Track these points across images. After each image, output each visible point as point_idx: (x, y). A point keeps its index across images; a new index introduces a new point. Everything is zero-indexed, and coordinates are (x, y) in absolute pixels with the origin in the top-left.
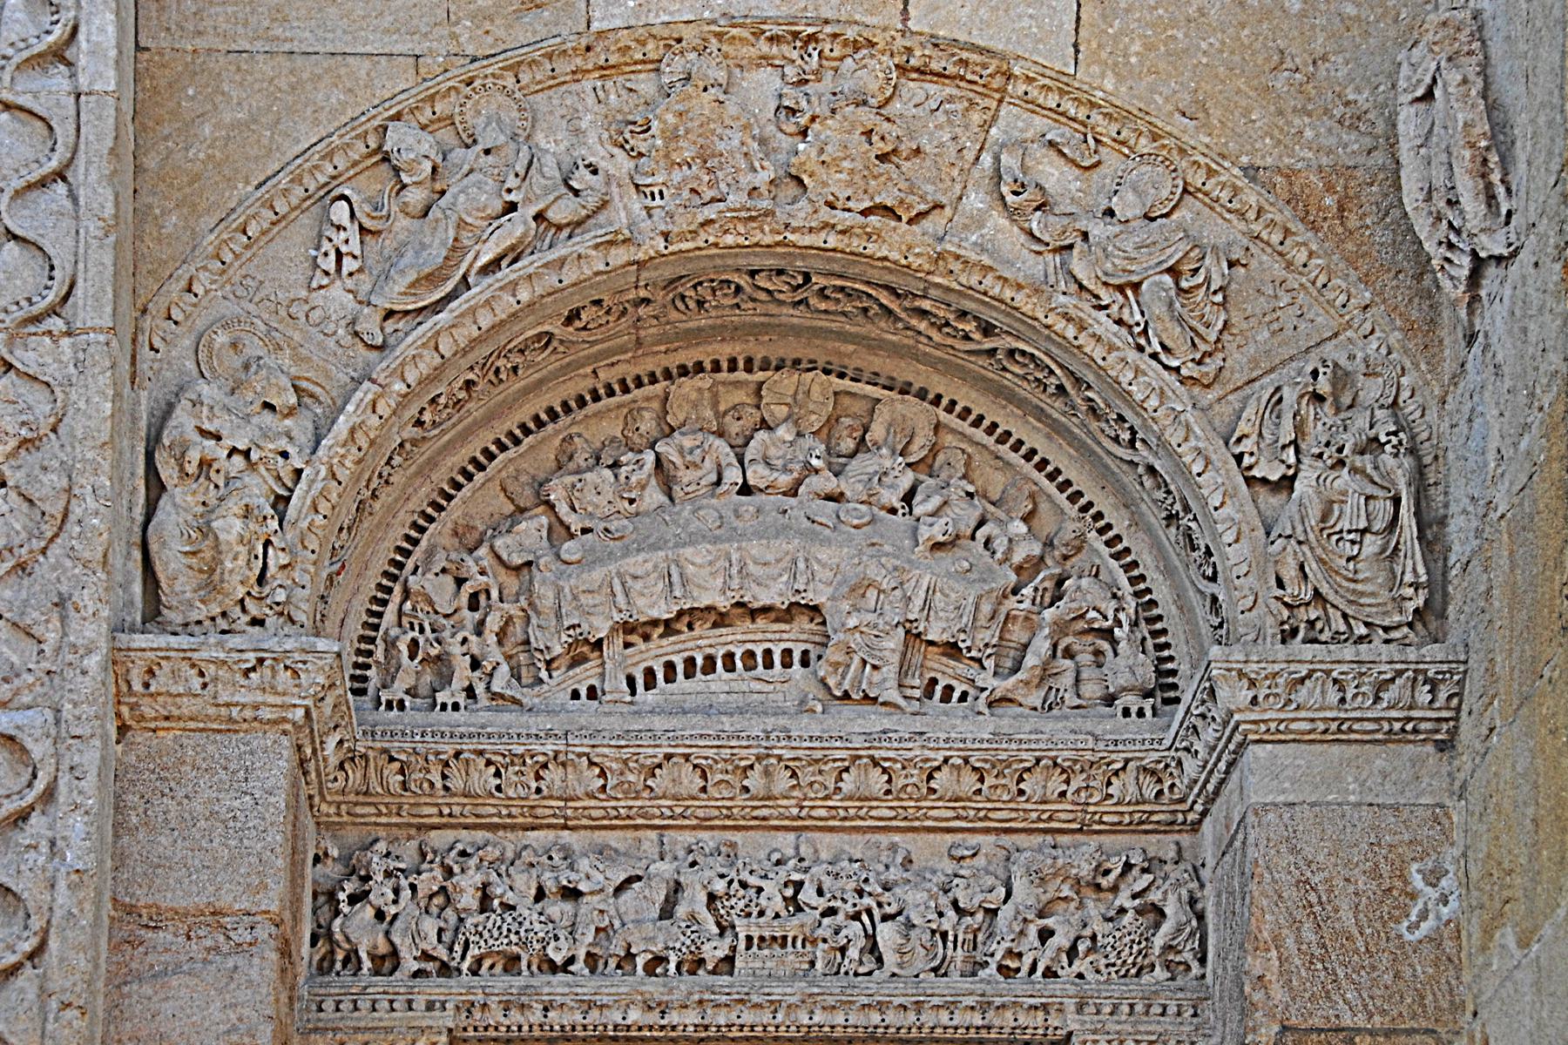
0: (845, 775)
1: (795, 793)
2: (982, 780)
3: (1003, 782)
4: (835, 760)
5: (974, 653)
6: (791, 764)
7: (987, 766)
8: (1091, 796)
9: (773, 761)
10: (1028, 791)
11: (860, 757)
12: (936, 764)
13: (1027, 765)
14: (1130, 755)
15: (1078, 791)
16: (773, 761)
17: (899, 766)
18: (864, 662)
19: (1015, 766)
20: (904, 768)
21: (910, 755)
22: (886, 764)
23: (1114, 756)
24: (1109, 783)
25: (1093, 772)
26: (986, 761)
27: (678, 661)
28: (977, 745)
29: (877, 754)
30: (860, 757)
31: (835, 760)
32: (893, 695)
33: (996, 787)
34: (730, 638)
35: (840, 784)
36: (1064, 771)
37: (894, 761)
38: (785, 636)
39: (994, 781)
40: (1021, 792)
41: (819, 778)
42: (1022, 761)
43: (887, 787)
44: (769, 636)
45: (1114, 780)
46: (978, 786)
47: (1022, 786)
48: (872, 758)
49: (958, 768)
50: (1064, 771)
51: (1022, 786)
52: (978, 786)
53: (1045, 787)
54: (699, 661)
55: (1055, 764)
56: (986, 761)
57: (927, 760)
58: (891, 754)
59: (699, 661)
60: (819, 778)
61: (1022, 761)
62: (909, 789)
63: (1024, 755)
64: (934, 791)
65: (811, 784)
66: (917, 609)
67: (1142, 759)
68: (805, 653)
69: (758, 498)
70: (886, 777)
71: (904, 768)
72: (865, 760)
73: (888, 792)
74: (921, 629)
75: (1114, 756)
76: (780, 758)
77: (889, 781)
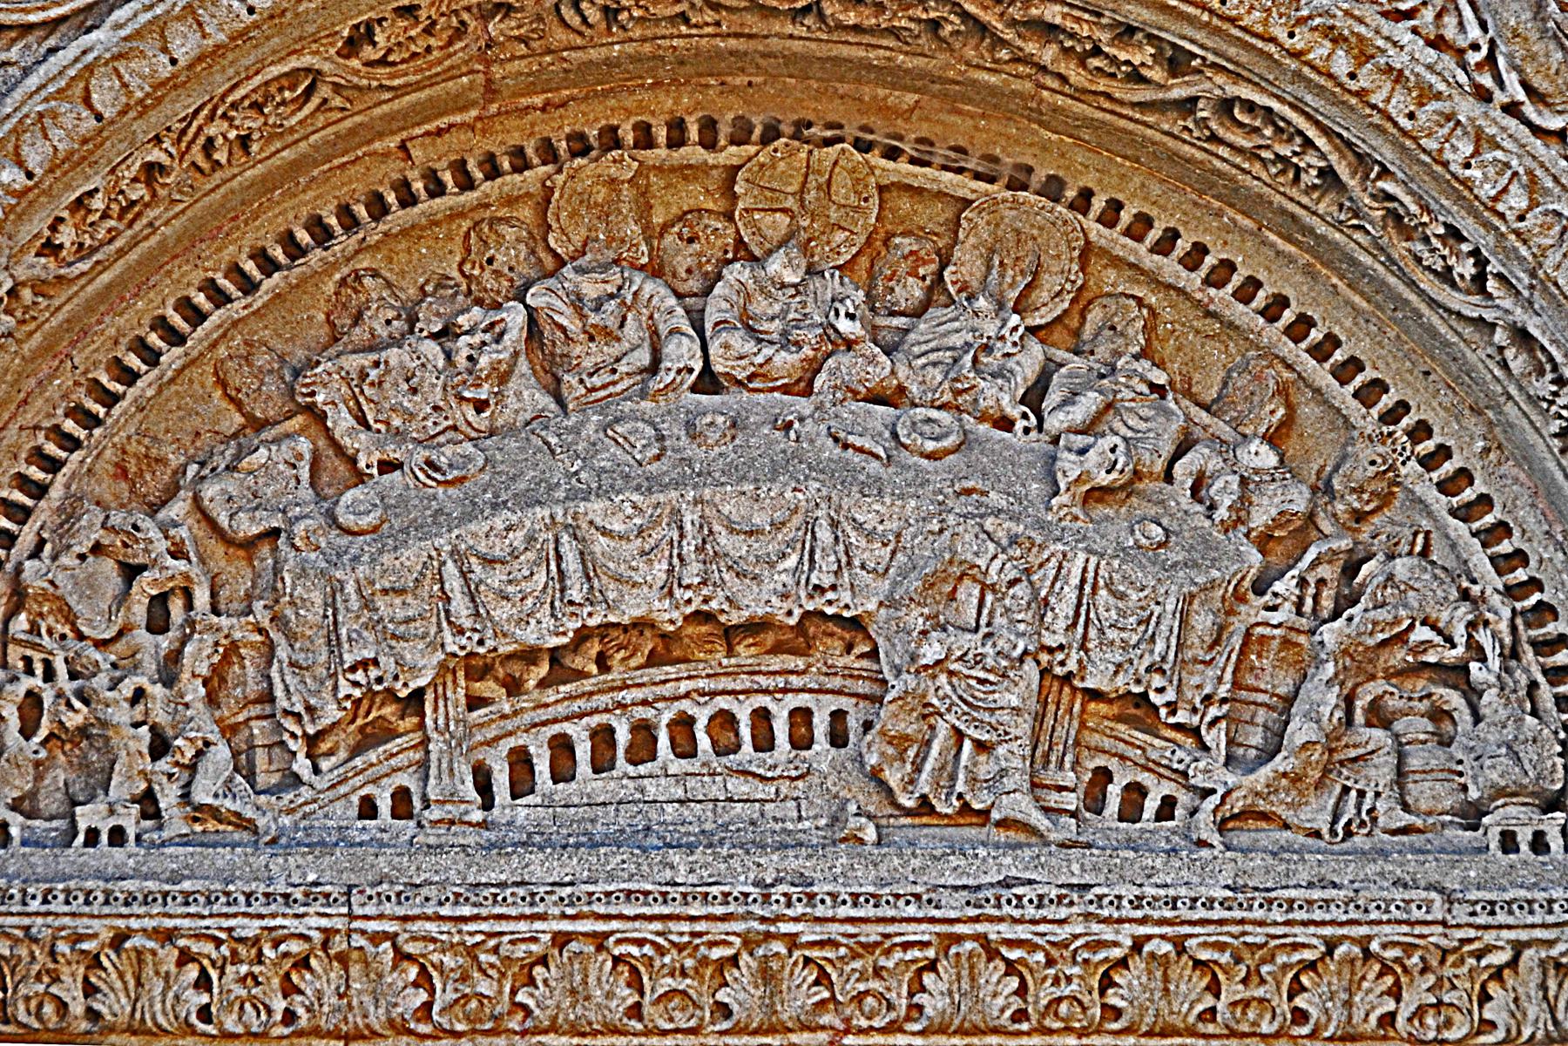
0: (928, 979)
1: (825, 1020)
2: (1214, 989)
3: (1260, 992)
4: (906, 946)
5: (1182, 717)
6: (815, 953)
7: (1225, 958)
8: (1448, 1024)
9: (779, 947)
10: (1314, 1013)
11: (959, 939)
12: (1117, 953)
13: (1308, 955)
14: (1524, 935)
15: (1420, 1012)
16: (779, 947)
17: (1040, 957)
18: (959, 735)
19: (1282, 959)
20: (1050, 962)
21: (1063, 933)
22: (1014, 955)
23: (1489, 937)
24: (1485, 998)
25: (1448, 971)
26: (1221, 947)
27: (578, 733)
28: (1201, 913)
29: (993, 931)
30: (959, 939)
31: (906, 946)
32: (1022, 806)
33: (1246, 1003)
34: (684, 686)
35: (920, 998)
36: (1386, 970)
37: (1032, 947)
38: (796, 681)
39: (1241, 992)
40: (1300, 1016)
41: (875, 985)
42: (1296, 947)
43: (1017, 1003)
44: (763, 681)
45: (1493, 988)
46: (1209, 1001)
47: (1300, 1002)
48: (982, 938)
49: (1164, 961)
50: (1386, 970)
51: (1300, 1002)
52: (1209, 1001)
53: (1348, 1004)
54: (623, 736)
55: (1368, 955)
56: (1221, 947)
57: (1101, 944)
58: (1022, 932)
59: (623, 736)
60: (875, 985)
61: (1296, 947)
62: (1063, 1008)
63: (1301, 935)
64: (1117, 1013)
65: (860, 998)
66: (1061, 624)
67: (1550, 943)
68: (838, 716)
69: (733, 399)
70: (1014, 983)
71: (1050, 962)
72: (969, 945)
73: (1021, 1015)
74: (1072, 666)
75: (1489, 937)
76: (792, 941)
77: (1022, 991)
